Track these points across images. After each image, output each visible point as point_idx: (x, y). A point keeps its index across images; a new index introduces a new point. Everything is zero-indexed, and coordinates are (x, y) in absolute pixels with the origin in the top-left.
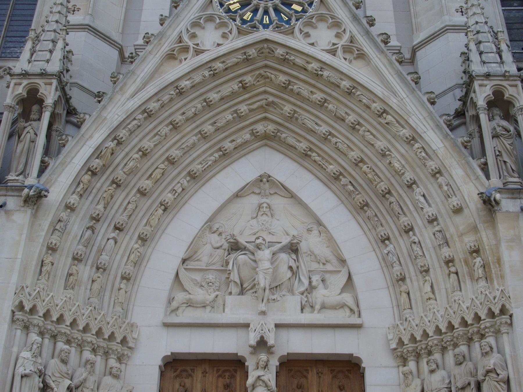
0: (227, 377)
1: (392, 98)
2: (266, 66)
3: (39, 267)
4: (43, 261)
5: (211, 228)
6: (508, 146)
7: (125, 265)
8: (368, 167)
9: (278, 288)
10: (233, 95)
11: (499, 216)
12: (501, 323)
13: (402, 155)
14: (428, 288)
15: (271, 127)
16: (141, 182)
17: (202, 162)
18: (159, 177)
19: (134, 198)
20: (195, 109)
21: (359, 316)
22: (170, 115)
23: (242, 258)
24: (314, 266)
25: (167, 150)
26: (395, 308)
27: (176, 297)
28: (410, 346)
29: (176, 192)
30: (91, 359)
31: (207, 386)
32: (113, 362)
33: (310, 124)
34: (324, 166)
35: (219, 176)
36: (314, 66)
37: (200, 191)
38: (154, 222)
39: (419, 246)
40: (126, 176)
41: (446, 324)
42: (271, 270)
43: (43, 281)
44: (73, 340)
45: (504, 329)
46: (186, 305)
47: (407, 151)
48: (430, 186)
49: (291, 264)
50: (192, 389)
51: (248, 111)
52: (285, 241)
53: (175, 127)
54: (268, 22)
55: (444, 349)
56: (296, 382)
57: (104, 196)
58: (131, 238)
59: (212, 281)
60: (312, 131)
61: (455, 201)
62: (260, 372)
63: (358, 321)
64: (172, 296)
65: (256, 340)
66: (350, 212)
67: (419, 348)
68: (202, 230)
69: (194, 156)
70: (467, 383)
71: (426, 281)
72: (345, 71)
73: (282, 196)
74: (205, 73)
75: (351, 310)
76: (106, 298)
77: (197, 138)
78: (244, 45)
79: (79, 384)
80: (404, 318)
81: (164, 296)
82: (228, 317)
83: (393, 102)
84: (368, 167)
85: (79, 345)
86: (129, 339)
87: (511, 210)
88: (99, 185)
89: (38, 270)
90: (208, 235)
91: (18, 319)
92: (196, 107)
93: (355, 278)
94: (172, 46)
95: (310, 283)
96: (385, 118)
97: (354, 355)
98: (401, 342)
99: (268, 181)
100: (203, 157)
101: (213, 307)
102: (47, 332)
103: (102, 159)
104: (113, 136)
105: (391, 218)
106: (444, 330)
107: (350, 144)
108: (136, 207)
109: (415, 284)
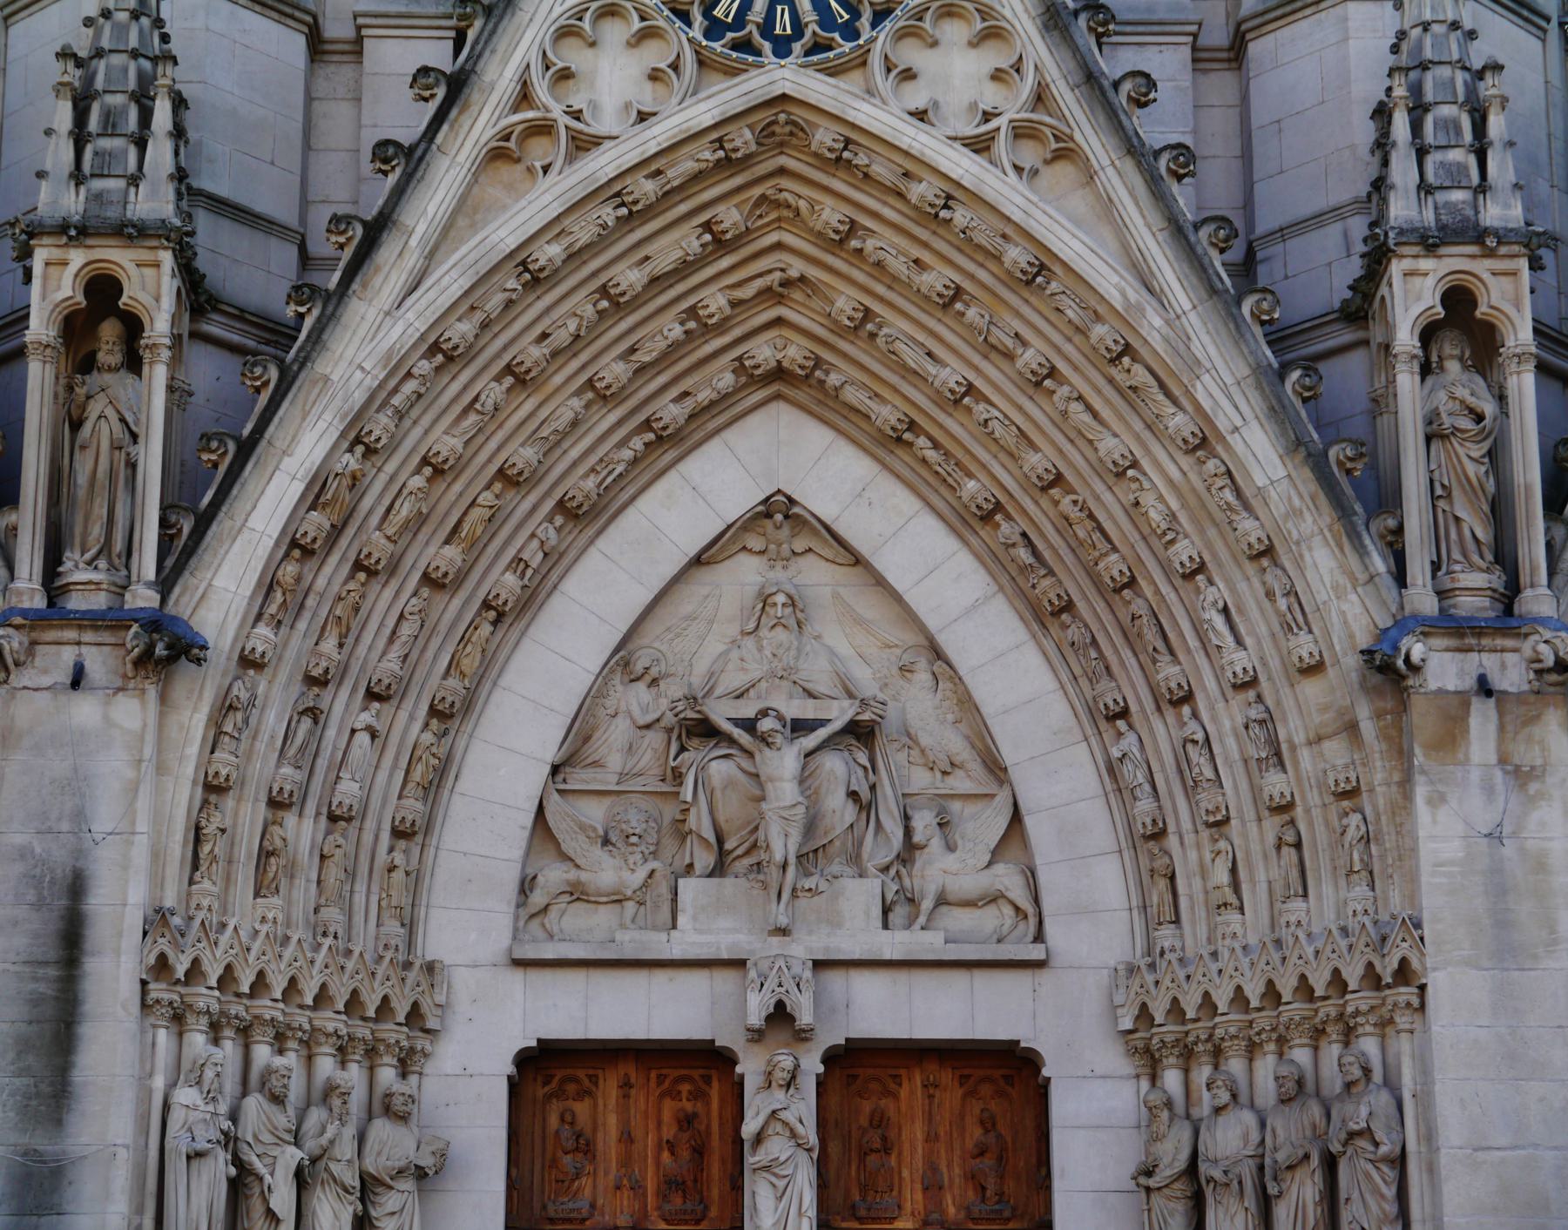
0: (684, 1095)
1: (1150, 312)
2: (782, 171)
3: (190, 847)
4: (198, 829)
5: (626, 664)
6: (1471, 468)
7: (400, 797)
8: (1075, 502)
9: (821, 851)
10: (685, 268)
11: (1418, 705)
12: (1395, 1005)
13: (1170, 482)
14: (1221, 876)
15: (795, 353)
16: (432, 550)
17: (598, 468)
18: (479, 532)
19: (414, 601)
20: (577, 320)
21: (1039, 937)
22: (505, 348)
23: (721, 770)
24: (921, 779)
25: (499, 449)
26: (1135, 913)
27: (540, 879)
28: (1171, 1030)
29: (527, 566)
30: (342, 1083)
31: (633, 1124)
32: (387, 1075)
33: (912, 357)
34: (950, 480)
35: (643, 503)
36: (923, 191)
37: (593, 550)
38: (470, 663)
39: (1205, 751)
40: (390, 546)
41: (1261, 988)
42: (801, 810)
43: (206, 884)
44: (290, 1034)
45: (1402, 1020)
46: (567, 898)
47: (1185, 474)
48: (1242, 586)
49: (854, 787)
50: (595, 1130)
51: (728, 311)
52: (840, 713)
53: (519, 378)
54: (789, 31)
55: (1252, 1050)
56: (867, 1107)
57: (338, 613)
58: (412, 718)
59: (637, 831)
60: (915, 372)
61: (1304, 646)
62: (778, 1097)
63: (1036, 953)
64: (530, 871)
65: (764, 1014)
66: (1022, 618)
67: (1191, 1039)
68: (605, 673)
69: (574, 453)
70: (1301, 1153)
71: (1219, 853)
72: (1017, 216)
73: (827, 560)
74: (604, 217)
75: (1017, 909)
76: (359, 899)
77: (583, 403)
78: (718, 119)
79: (317, 1152)
80: (1158, 951)
81: (511, 876)
82: (684, 943)
83: (1153, 325)
84: (1075, 502)
85: (306, 1044)
86: (426, 1007)
87: (1451, 687)
88: (321, 582)
89: (189, 854)
90: (620, 688)
91: (158, 1001)
92: (581, 318)
93: (1029, 821)
94: (504, 122)
95: (908, 832)
96: (1129, 371)
97: (1023, 1045)
98: (1144, 1014)
99: (786, 517)
100: (600, 452)
101: (640, 904)
102: (229, 1022)
103: (328, 510)
104: (352, 435)
105: (1136, 654)
106: (1254, 1003)
107: (1026, 426)
108: (422, 626)
109: (1193, 855)
